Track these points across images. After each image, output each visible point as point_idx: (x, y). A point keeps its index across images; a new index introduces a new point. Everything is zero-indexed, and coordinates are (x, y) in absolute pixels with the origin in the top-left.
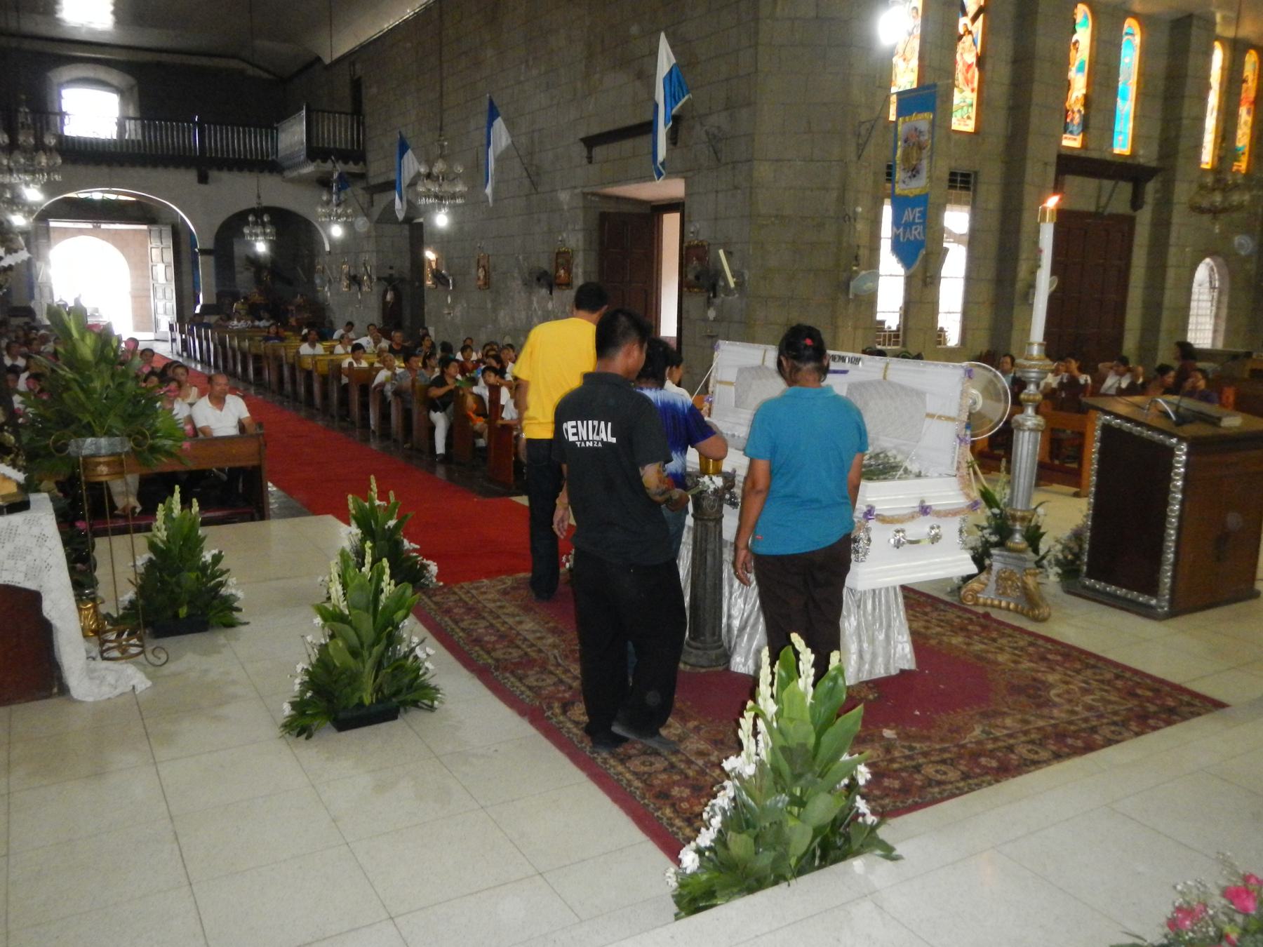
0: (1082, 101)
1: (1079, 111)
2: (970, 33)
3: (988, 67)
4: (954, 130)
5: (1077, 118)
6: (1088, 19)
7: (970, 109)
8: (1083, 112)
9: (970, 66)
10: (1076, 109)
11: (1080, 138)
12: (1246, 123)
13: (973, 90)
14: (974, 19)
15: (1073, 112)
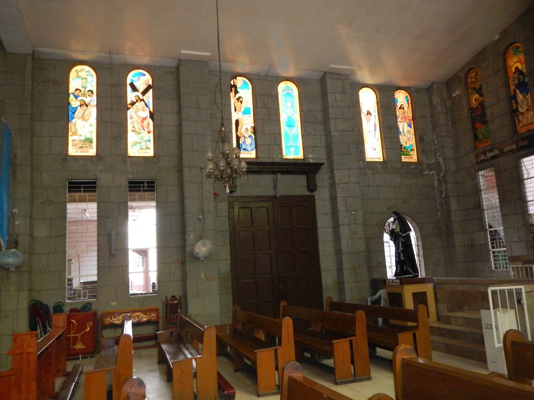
0: (250, 130)
1: (250, 136)
2: (143, 100)
3: (155, 117)
4: (129, 157)
5: (249, 141)
6: (248, 84)
7: (148, 143)
8: (254, 137)
9: (144, 119)
10: (247, 136)
11: (254, 153)
12: (409, 132)
13: (149, 132)
14: (144, 93)
15: (245, 137)
